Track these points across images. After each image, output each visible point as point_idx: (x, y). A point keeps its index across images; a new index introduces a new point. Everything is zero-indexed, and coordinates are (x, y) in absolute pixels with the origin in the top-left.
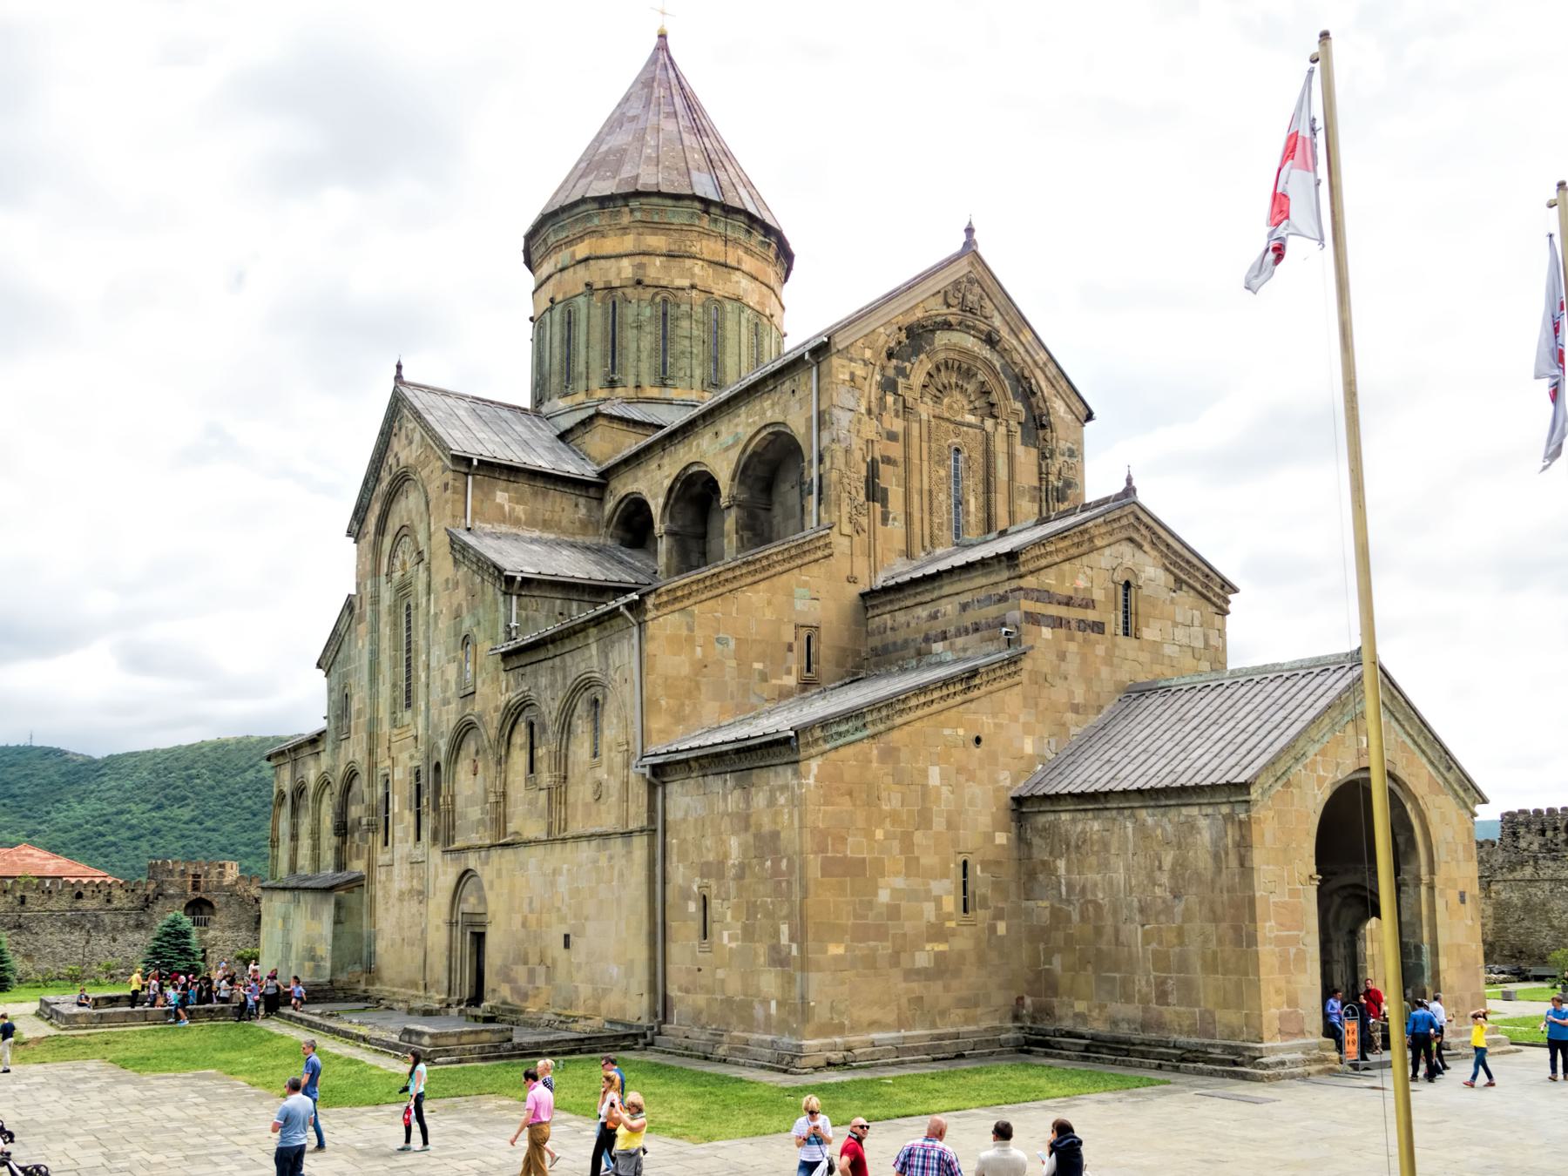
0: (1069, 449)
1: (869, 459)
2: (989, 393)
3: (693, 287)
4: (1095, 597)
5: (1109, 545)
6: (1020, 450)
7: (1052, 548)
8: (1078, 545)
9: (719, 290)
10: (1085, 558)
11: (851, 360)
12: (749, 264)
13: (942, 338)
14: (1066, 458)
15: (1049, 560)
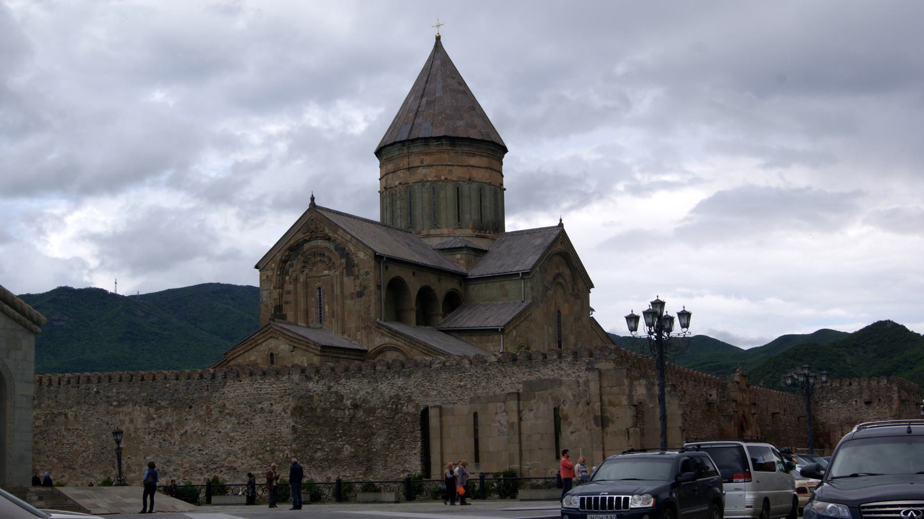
0: (366, 272)
1: (274, 306)
2: (330, 259)
3: (400, 184)
4: (258, 362)
5: (263, 342)
6: (345, 279)
7: (240, 349)
8: (250, 345)
9: (411, 180)
10: (254, 349)
11: (267, 270)
12: (428, 160)
13: (307, 246)
14: (364, 276)
15: (239, 353)
